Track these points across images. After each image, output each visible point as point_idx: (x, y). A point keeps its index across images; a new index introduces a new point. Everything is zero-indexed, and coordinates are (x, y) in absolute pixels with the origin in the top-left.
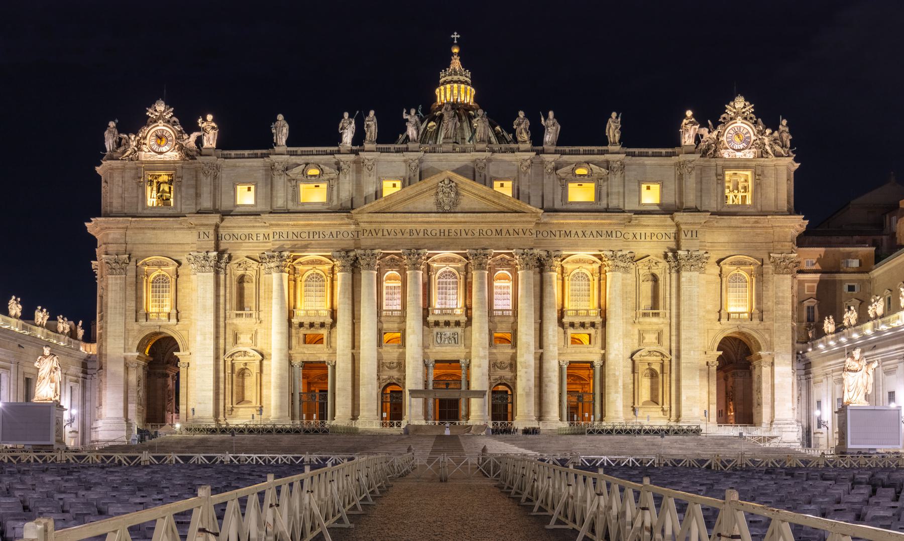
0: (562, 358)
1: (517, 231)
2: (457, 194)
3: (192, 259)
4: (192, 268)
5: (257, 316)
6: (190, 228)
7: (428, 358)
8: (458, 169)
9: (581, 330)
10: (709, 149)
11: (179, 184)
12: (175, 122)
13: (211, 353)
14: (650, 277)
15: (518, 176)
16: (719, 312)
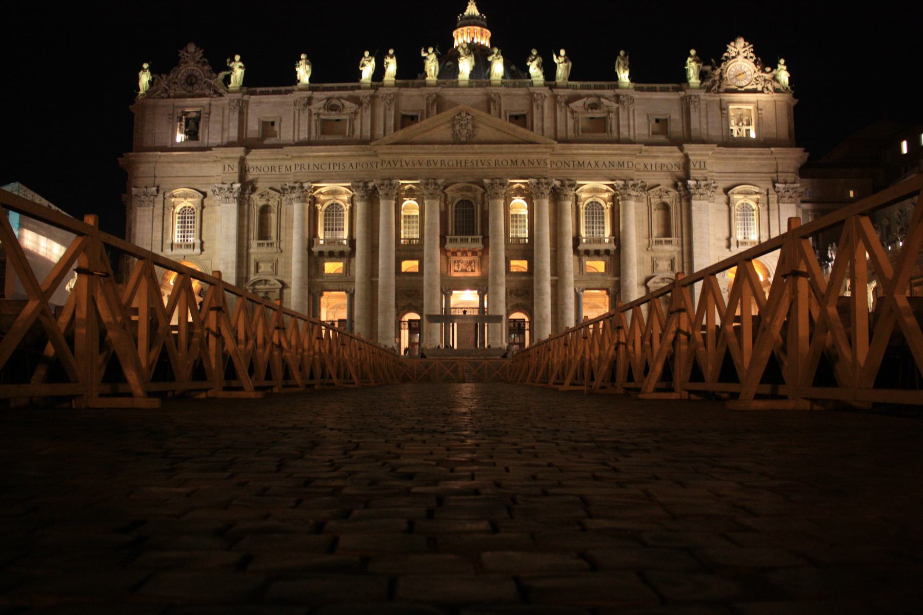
0: (578, 285)
3: (217, 191)
6: (215, 161)
10: (713, 85)
11: (207, 119)
12: (204, 62)
16: (729, 239)
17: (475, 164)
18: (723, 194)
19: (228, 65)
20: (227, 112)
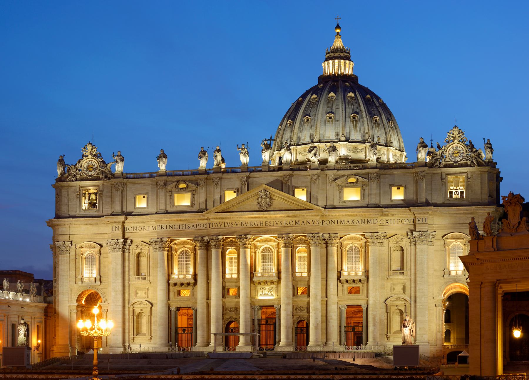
1: (309, 222)
2: (271, 198)
5: (148, 279)
7: (254, 305)
10: (436, 162)
13: (120, 303)
14: (400, 248)
17: (272, 225)
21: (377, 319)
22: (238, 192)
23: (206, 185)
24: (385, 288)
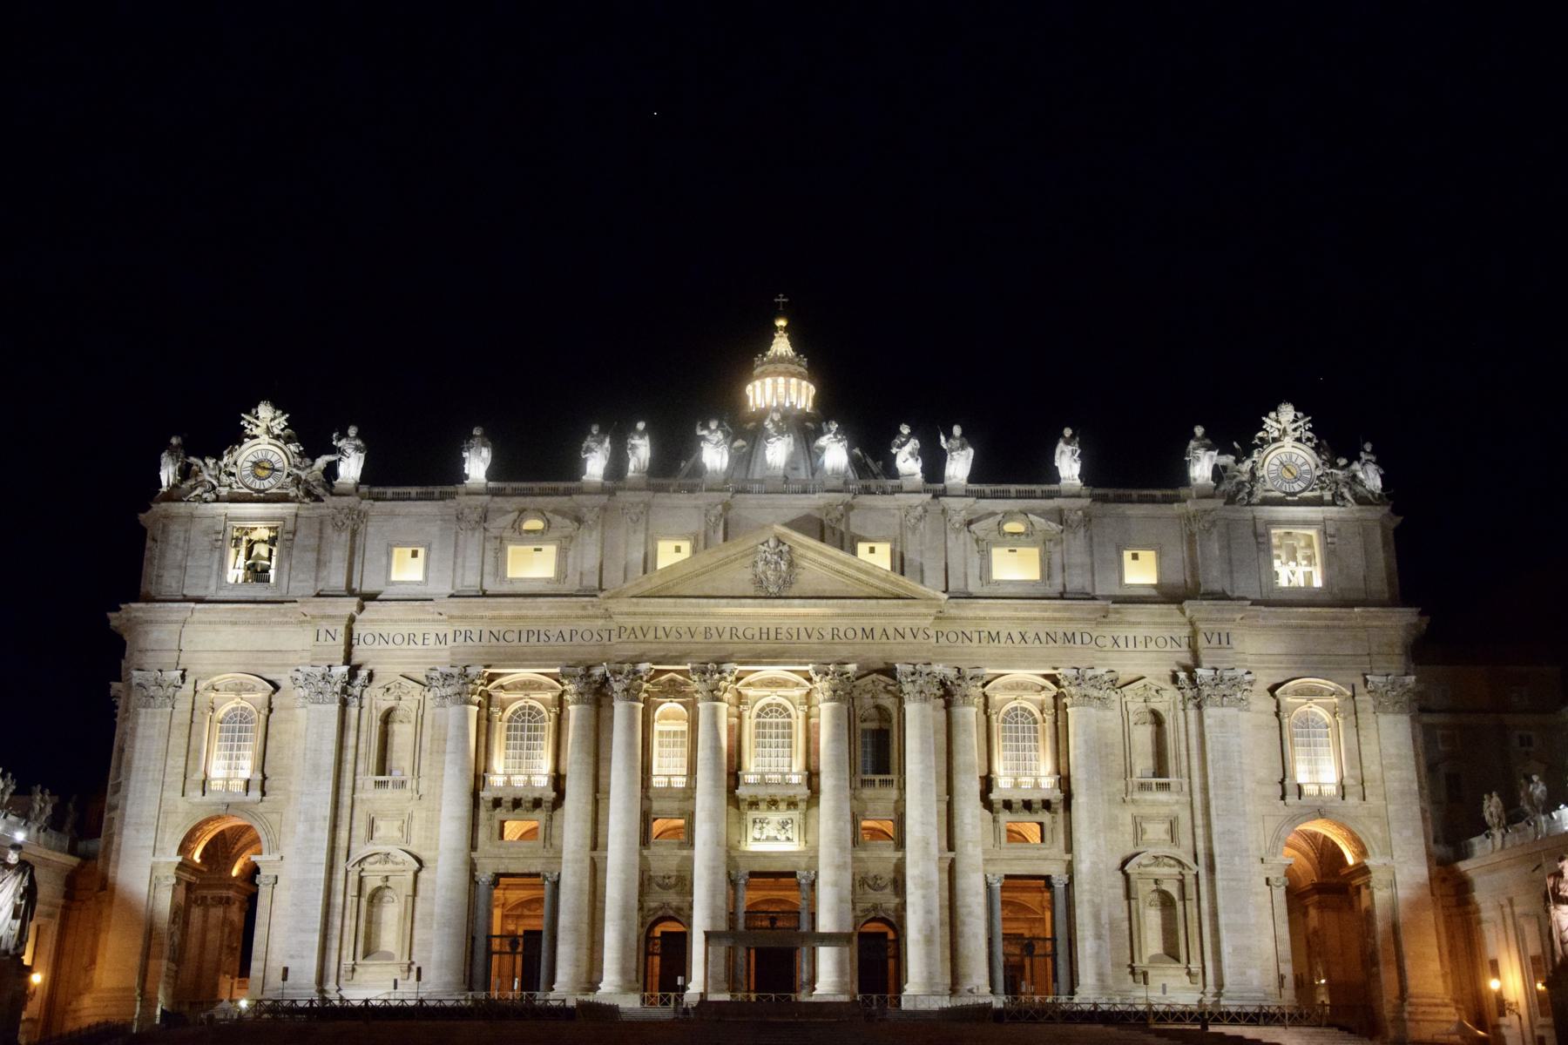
0: (991, 869)
1: (902, 632)
2: (791, 564)
4: (300, 697)
5: (414, 787)
6: (302, 622)
7: (737, 867)
8: (793, 521)
9: (1026, 816)
10: (1239, 491)
13: (323, 857)
14: (1149, 717)
15: (901, 535)
16: (1282, 782)
18: (1268, 694)
19: (334, 443)
20: (329, 530)
21: (1104, 919)
22: (701, 543)
23: (603, 526)
24: (1121, 828)
